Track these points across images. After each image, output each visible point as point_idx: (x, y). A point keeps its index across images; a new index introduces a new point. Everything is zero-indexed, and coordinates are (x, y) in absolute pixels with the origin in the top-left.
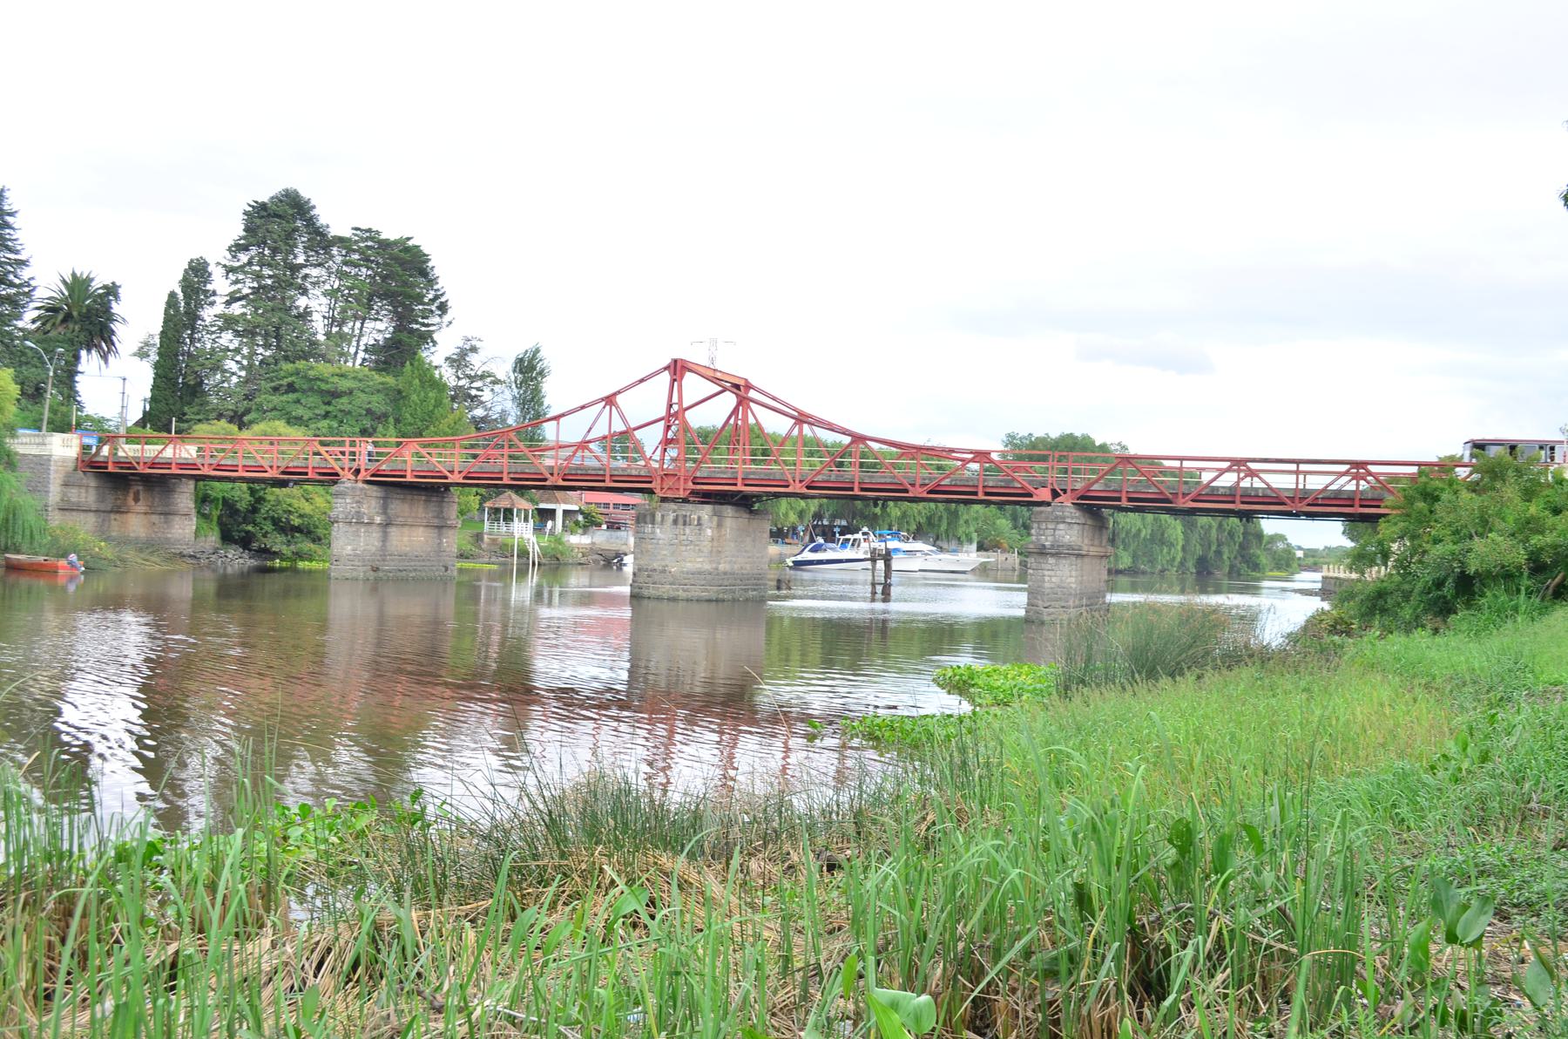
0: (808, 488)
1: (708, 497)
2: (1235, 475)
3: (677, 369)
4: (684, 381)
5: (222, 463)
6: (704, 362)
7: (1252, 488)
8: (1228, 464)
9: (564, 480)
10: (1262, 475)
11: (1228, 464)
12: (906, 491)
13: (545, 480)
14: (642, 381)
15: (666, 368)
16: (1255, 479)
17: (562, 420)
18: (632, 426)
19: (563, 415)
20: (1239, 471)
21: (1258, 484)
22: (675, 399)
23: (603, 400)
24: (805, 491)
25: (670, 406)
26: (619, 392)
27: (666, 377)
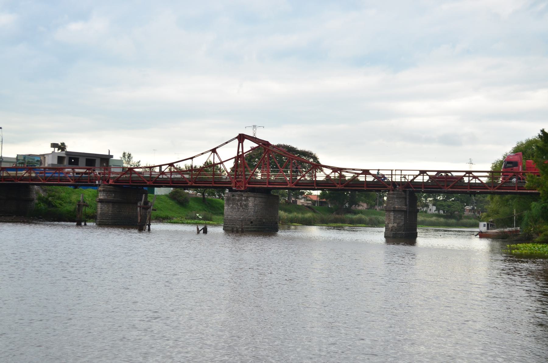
0: (295, 185)
1: (253, 190)
2: (468, 178)
3: (241, 138)
4: (244, 143)
5: (51, 178)
6: (252, 135)
7: (476, 183)
8: (465, 173)
9: (195, 183)
10: (479, 178)
11: (465, 173)
12: (336, 186)
13: (187, 183)
14: (227, 143)
15: (236, 138)
16: (477, 179)
17: (194, 159)
18: (223, 161)
19: (194, 157)
20: (469, 177)
21: (478, 181)
22: (240, 150)
23: (211, 150)
24: (294, 187)
25: (238, 152)
26: (217, 147)
27: (237, 141)
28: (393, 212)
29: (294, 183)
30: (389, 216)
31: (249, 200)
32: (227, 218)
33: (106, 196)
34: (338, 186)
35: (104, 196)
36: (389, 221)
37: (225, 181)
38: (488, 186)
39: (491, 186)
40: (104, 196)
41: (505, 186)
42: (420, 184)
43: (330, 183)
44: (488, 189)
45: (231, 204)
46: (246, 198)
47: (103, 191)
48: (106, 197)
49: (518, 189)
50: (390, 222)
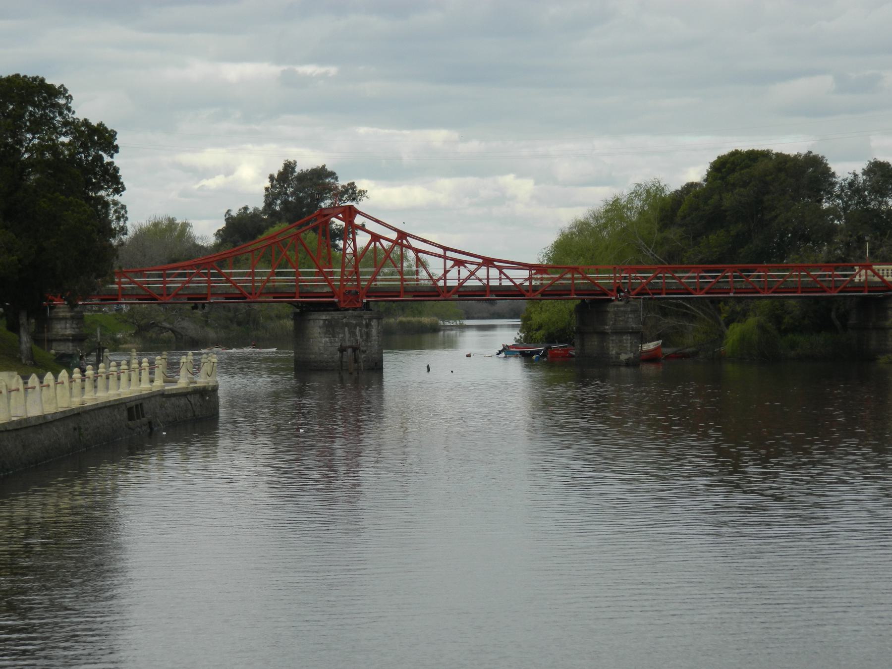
28: (629, 335)
29: (451, 291)
30: (621, 341)
31: (373, 324)
32: (333, 358)
33: (77, 328)
34: (528, 294)
35: (74, 328)
36: (621, 350)
37: (321, 291)
38: (760, 288)
39: (764, 289)
40: (74, 328)
41: (783, 288)
42: (660, 288)
43: (514, 291)
44: (759, 293)
45: (340, 333)
46: (367, 321)
47: (72, 318)
48: (77, 330)
49: (802, 292)
50: (621, 351)
